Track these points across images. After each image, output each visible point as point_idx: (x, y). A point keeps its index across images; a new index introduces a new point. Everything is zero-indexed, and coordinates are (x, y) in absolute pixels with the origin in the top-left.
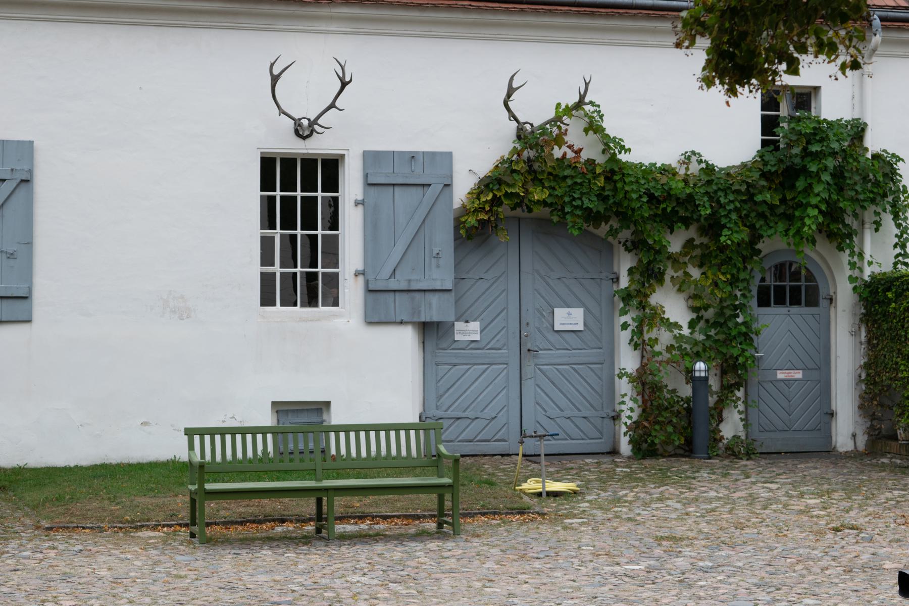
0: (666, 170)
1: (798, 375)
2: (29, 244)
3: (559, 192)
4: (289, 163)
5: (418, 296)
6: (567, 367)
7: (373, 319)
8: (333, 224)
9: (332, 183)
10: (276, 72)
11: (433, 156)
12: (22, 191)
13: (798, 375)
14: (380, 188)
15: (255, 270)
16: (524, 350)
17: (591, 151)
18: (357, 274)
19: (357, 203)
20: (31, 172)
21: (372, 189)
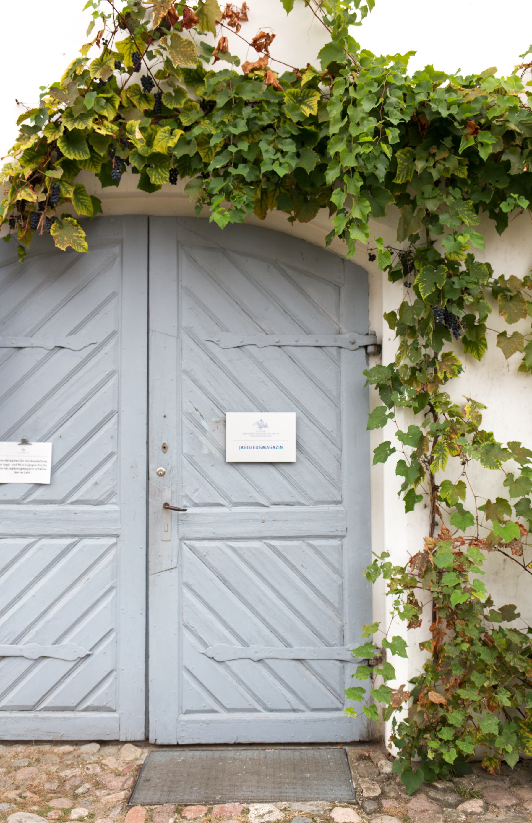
6: (257, 544)
16: (156, 505)
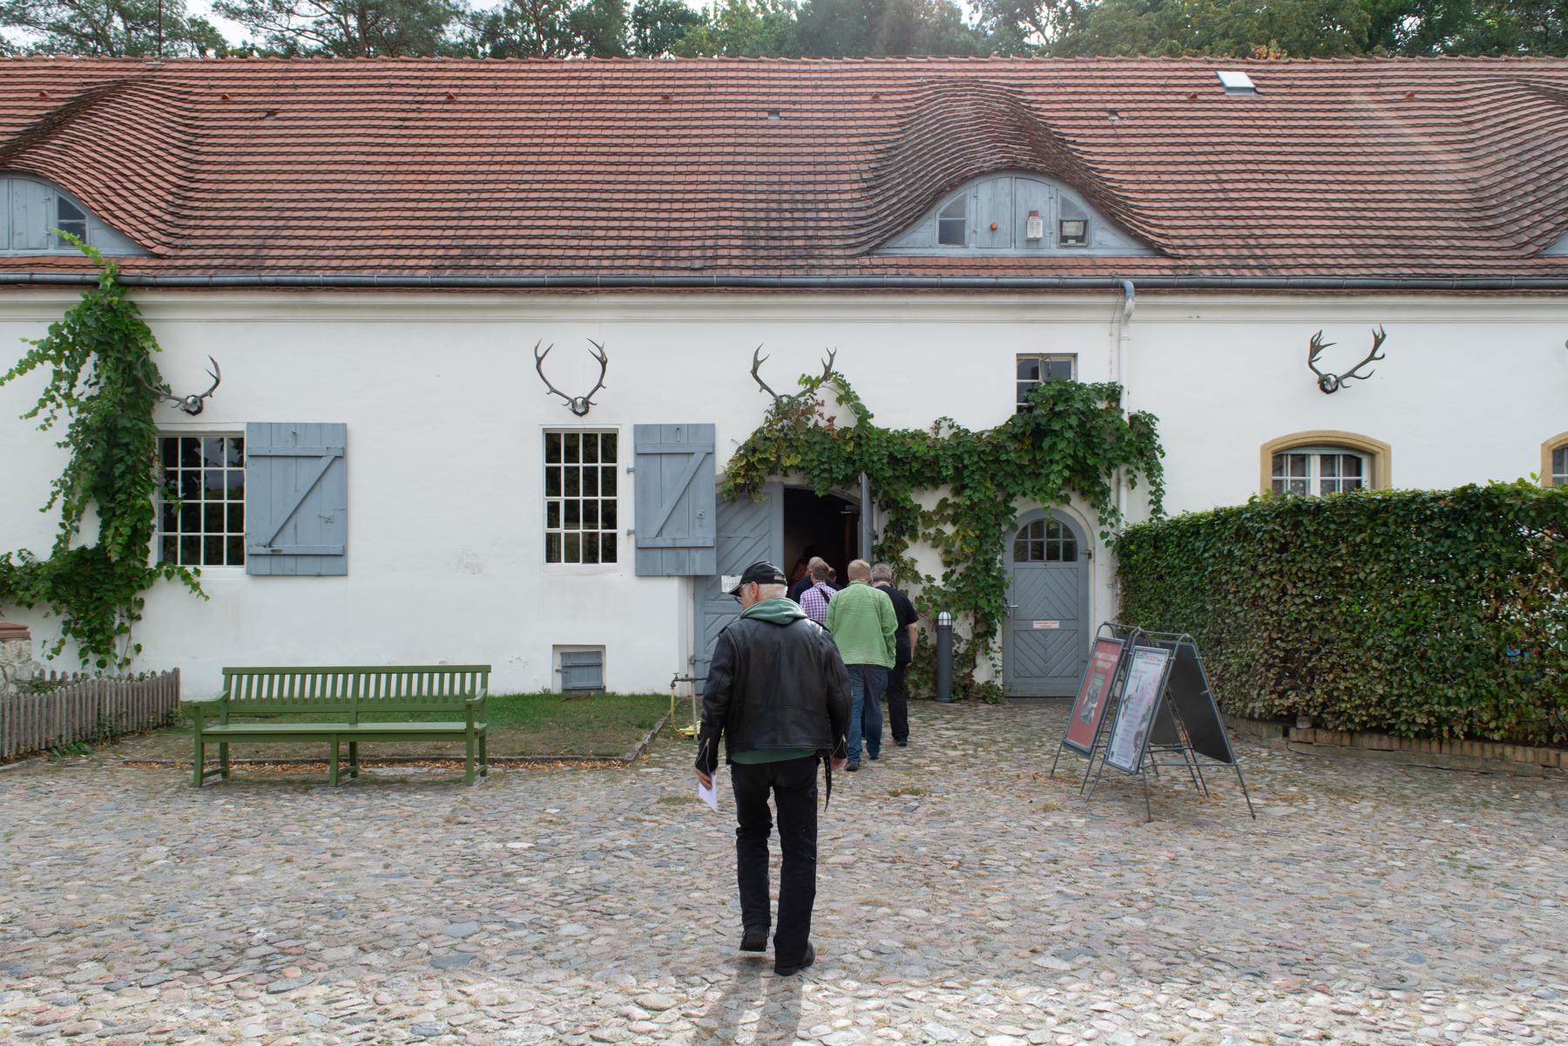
0: (919, 436)
1: (1055, 625)
2: (344, 510)
3: (811, 456)
4: (572, 437)
5: (682, 552)
7: (644, 572)
8: (611, 487)
9: (610, 453)
10: (540, 355)
11: (697, 427)
12: (338, 465)
13: (1055, 625)
14: (647, 458)
15: (540, 528)
17: (844, 419)
18: (629, 533)
19: (629, 471)
20: (344, 450)
21: (642, 458)
